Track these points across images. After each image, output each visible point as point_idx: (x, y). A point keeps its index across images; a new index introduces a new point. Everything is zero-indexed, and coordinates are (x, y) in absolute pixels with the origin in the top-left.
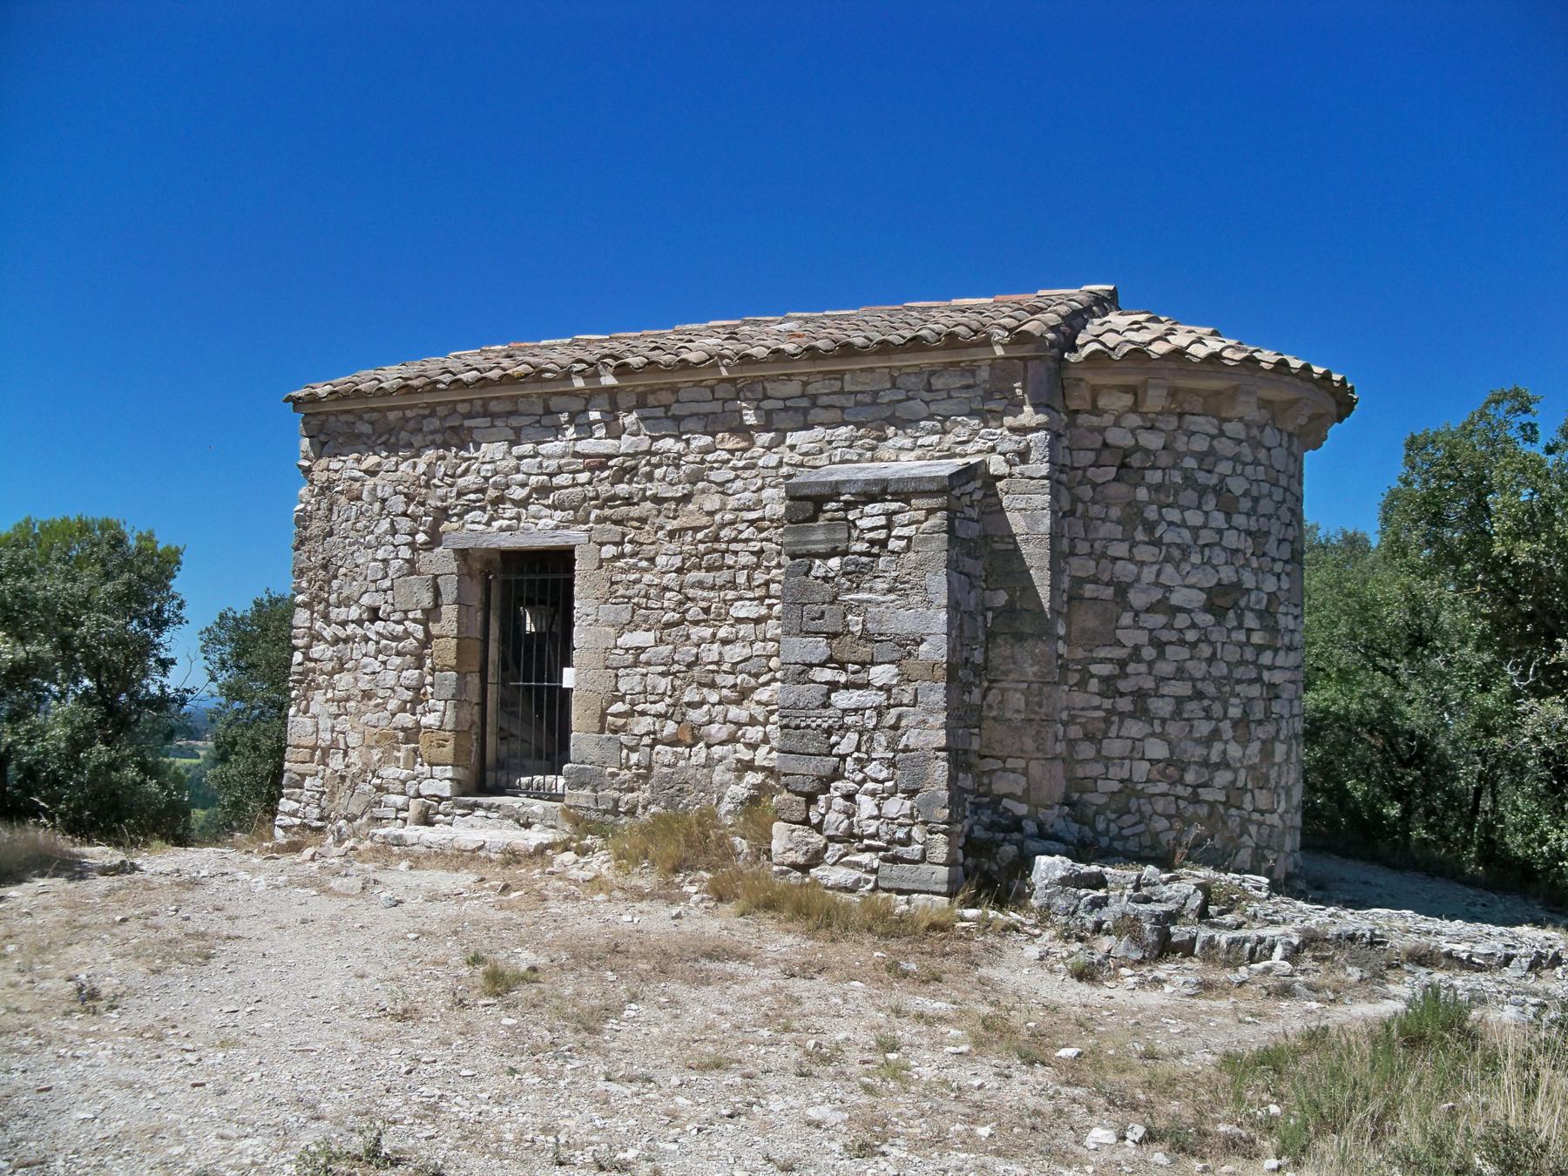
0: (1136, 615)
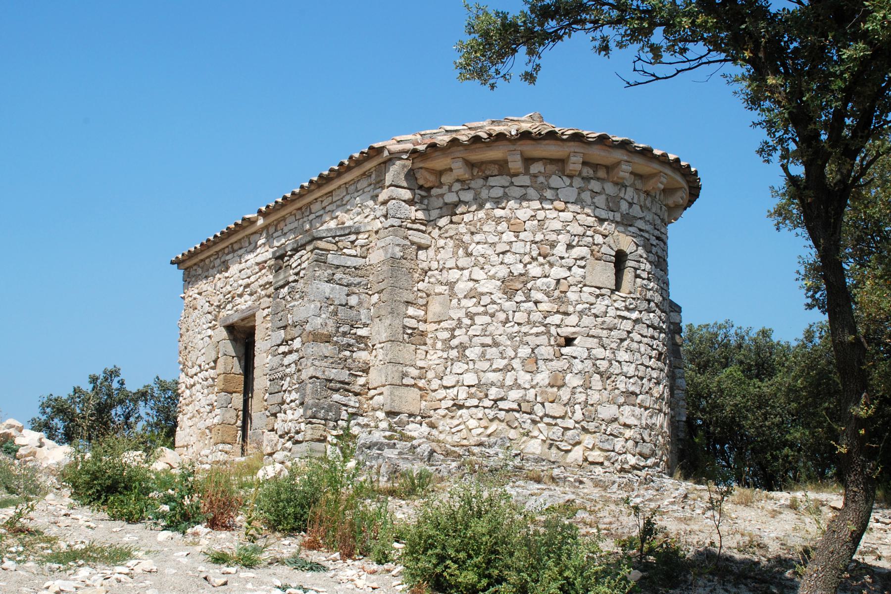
0: (459, 300)
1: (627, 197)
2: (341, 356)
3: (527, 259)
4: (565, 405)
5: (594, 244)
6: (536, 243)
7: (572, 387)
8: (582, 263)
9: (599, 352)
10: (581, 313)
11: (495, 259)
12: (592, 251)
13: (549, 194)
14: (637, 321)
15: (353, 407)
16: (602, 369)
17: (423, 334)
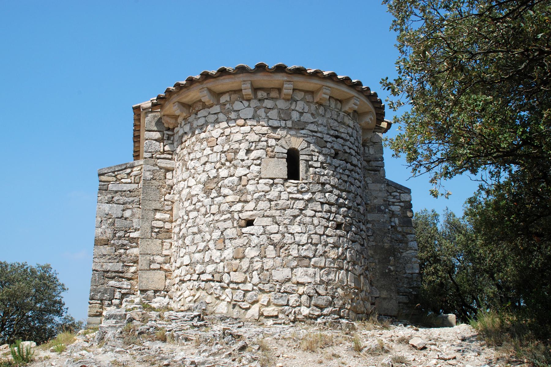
1: (297, 109)
2: (116, 253)
3: (218, 165)
4: (245, 273)
5: (268, 147)
6: (225, 152)
7: (250, 257)
8: (258, 162)
9: (274, 228)
10: (258, 200)
11: (200, 169)
12: (267, 152)
13: (233, 115)
14: (310, 200)
15: (125, 289)
16: (276, 241)
17: (168, 231)
